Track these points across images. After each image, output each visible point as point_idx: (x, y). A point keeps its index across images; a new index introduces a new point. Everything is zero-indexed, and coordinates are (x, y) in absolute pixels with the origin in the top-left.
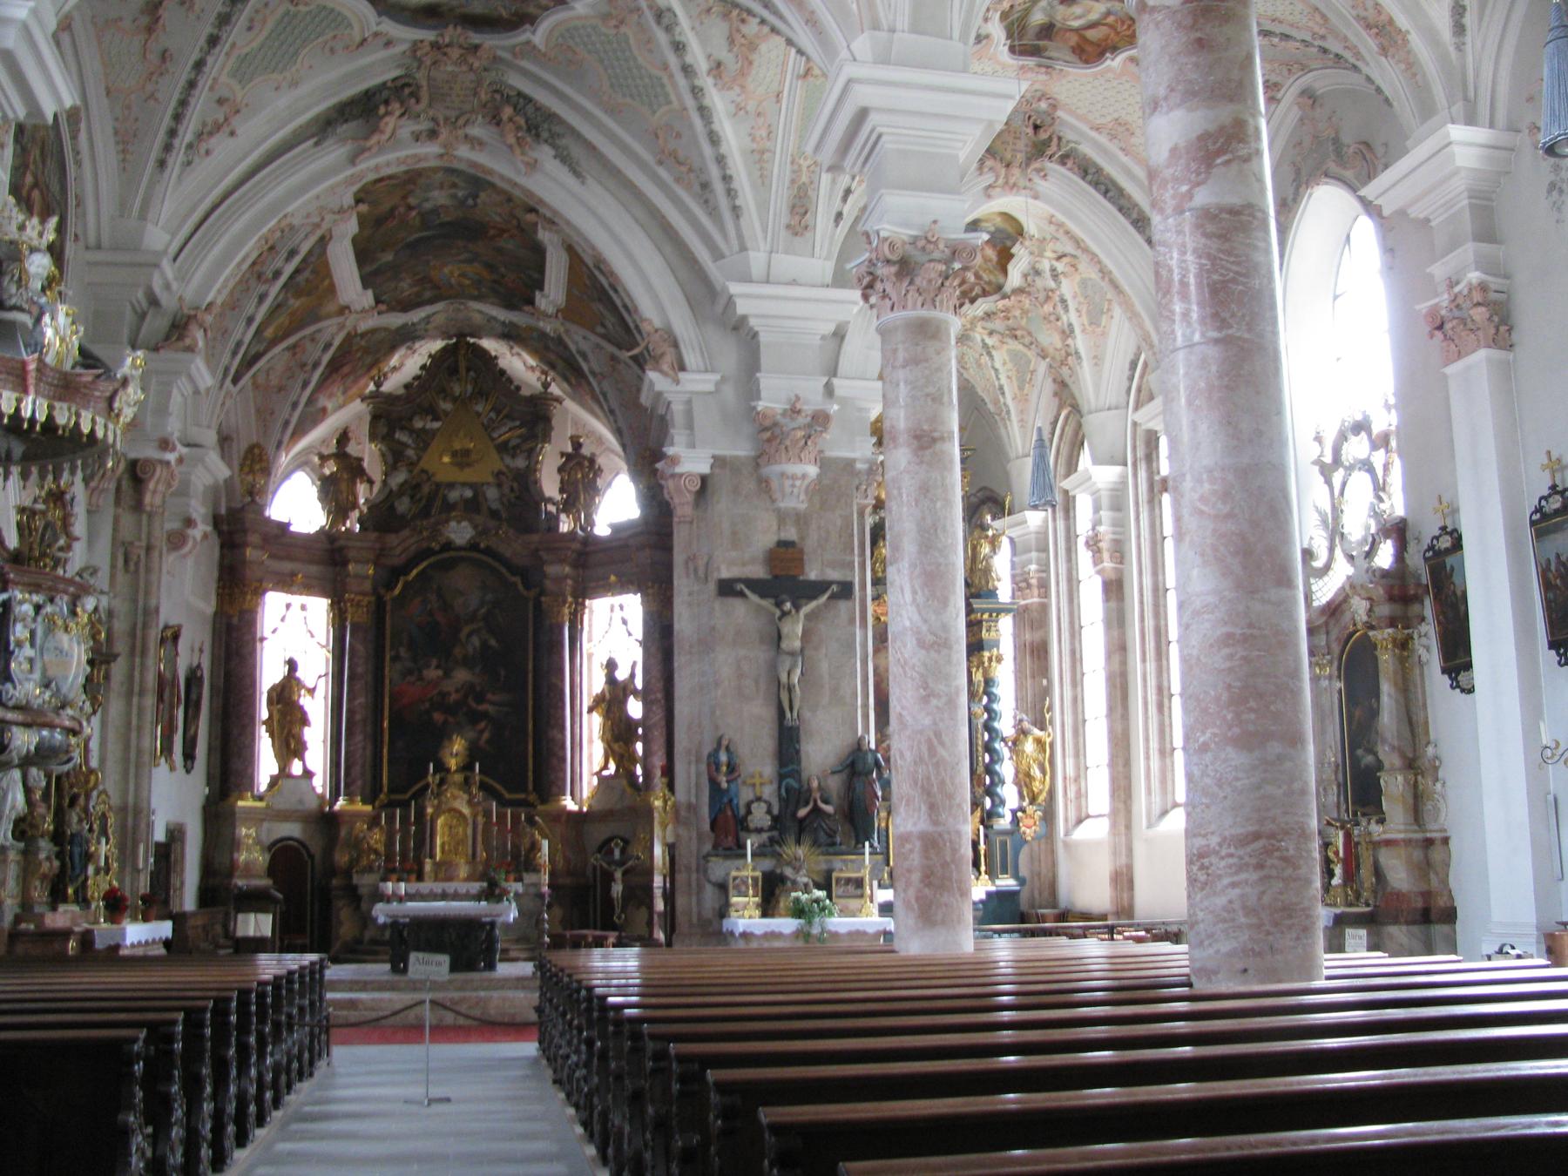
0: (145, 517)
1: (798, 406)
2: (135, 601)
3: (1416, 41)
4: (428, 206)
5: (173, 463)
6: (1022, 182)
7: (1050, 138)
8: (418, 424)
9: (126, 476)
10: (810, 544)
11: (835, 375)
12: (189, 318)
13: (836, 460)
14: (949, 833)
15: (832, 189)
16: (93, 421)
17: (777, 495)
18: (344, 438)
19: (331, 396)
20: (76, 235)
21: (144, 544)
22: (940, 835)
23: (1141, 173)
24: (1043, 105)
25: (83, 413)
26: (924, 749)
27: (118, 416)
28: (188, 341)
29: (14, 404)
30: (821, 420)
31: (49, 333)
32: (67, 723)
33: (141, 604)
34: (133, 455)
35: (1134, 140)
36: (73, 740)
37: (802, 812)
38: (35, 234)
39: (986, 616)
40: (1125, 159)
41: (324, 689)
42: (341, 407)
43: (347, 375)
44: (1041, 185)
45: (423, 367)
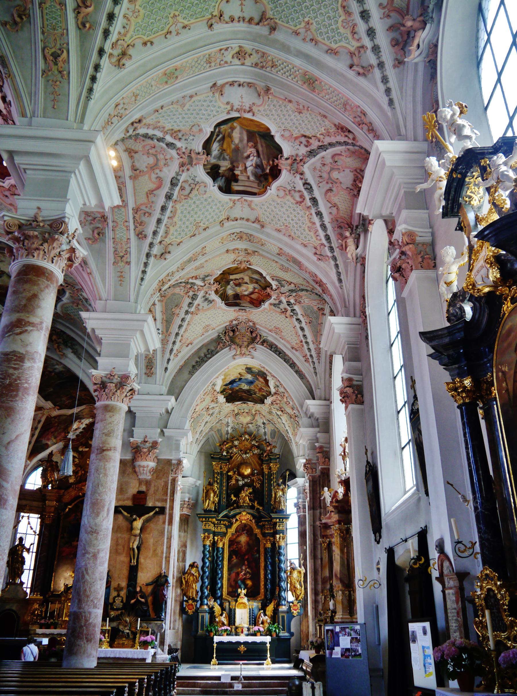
1: (146, 440)
3: (330, 286)
4: (57, 371)
6: (247, 353)
7: (257, 335)
8: (81, 449)
10: (151, 491)
11: (166, 427)
13: (161, 459)
14: (85, 612)
15: (162, 359)
17: (139, 474)
18: (51, 454)
19: (48, 439)
22: (81, 613)
23: (289, 347)
24: (251, 324)
26: (80, 575)
30: (155, 445)
35: (283, 334)
37: (133, 601)
39: (278, 520)
40: (283, 341)
41: (34, 548)
42: (56, 444)
43: (55, 432)
44: (254, 353)
45: (84, 429)
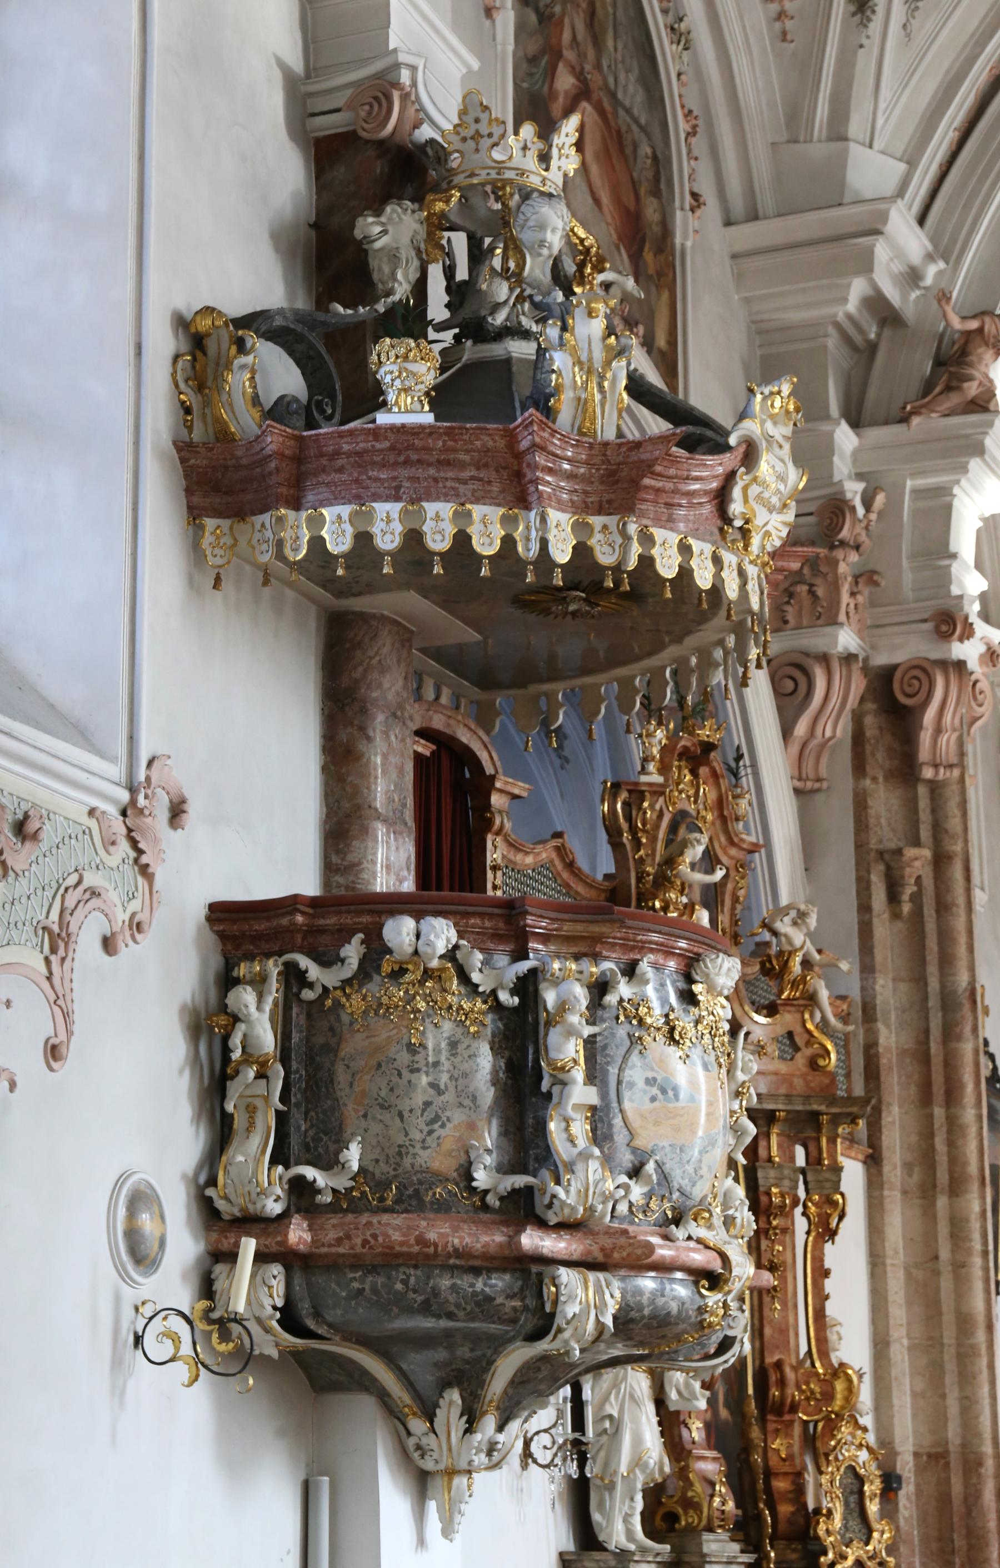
0: (922, 791)
2: (920, 980)
5: (973, 664)
9: (870, 706)
12: (968, 336)
16: (685, 549)
20: (695, 195)
21: (927, 853)
25: (659, 534)
27: (745, 533)
28: (972, 389)
29: (499, 532)
31: (559, 360)
32: (699, 1258)
33: (934, 983)
34: (881, 659)
36: (713, 1299)
38: (531, 162)
